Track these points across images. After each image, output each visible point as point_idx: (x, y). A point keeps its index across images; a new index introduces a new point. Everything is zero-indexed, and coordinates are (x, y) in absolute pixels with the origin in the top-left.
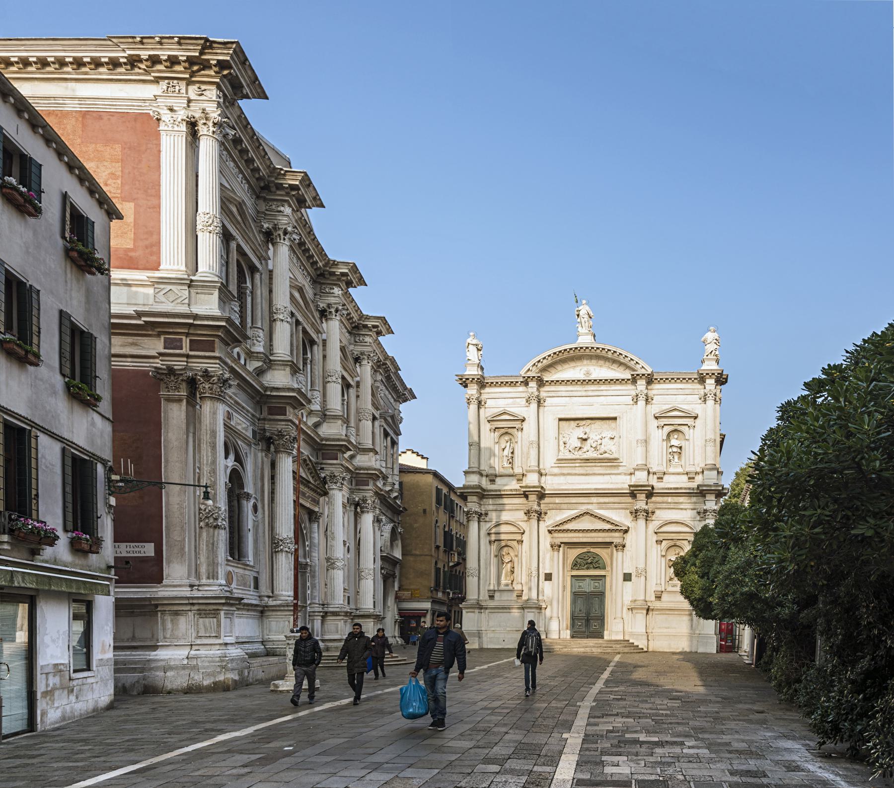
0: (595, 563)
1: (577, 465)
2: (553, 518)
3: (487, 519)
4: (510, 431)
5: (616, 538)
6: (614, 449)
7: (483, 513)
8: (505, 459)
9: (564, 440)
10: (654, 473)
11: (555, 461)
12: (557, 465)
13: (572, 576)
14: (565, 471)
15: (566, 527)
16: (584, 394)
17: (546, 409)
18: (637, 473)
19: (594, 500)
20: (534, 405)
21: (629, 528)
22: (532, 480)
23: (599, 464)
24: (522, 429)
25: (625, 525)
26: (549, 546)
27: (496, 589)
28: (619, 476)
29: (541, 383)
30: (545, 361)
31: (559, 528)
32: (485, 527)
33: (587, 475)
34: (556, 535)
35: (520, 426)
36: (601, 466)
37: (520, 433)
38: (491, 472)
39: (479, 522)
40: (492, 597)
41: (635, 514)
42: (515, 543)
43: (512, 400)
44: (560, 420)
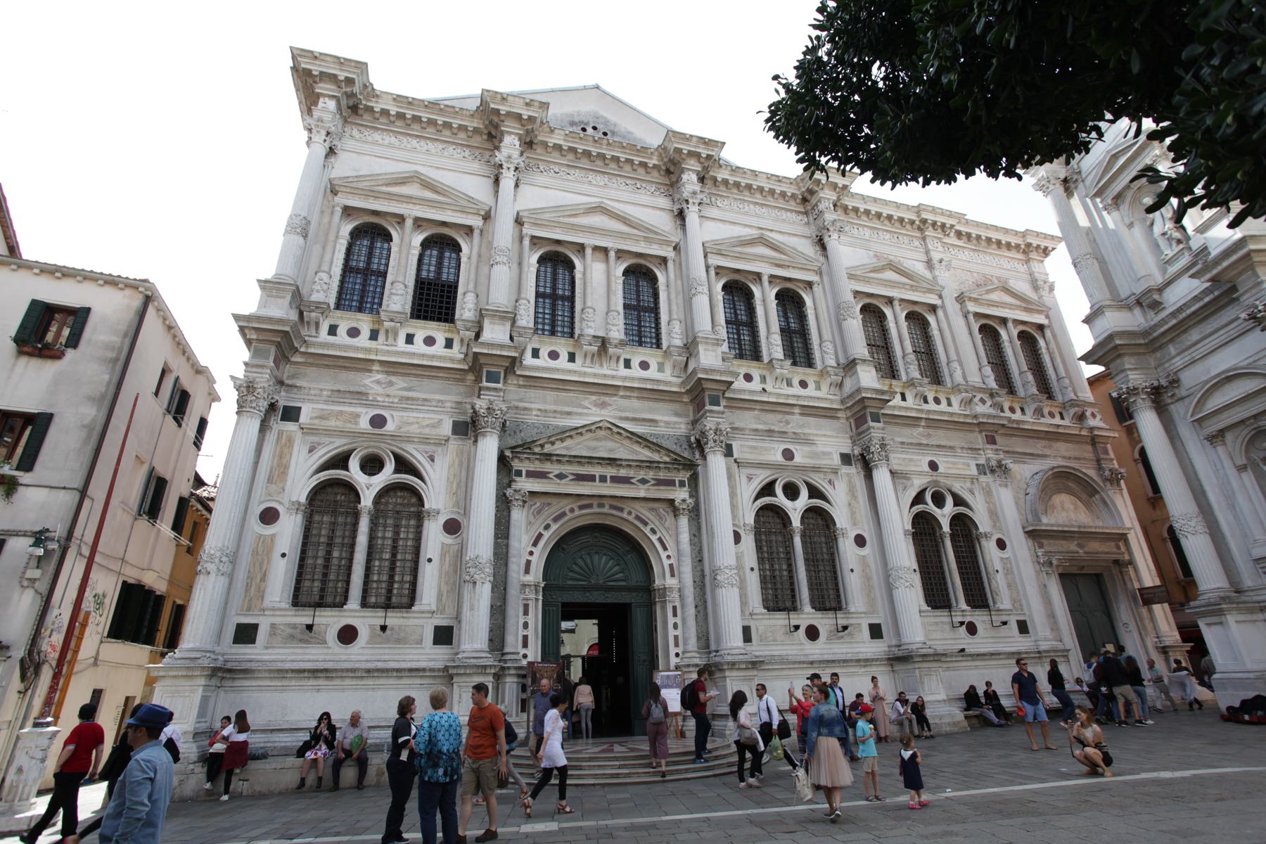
7: (1164, 382)
32: (1181, 412)
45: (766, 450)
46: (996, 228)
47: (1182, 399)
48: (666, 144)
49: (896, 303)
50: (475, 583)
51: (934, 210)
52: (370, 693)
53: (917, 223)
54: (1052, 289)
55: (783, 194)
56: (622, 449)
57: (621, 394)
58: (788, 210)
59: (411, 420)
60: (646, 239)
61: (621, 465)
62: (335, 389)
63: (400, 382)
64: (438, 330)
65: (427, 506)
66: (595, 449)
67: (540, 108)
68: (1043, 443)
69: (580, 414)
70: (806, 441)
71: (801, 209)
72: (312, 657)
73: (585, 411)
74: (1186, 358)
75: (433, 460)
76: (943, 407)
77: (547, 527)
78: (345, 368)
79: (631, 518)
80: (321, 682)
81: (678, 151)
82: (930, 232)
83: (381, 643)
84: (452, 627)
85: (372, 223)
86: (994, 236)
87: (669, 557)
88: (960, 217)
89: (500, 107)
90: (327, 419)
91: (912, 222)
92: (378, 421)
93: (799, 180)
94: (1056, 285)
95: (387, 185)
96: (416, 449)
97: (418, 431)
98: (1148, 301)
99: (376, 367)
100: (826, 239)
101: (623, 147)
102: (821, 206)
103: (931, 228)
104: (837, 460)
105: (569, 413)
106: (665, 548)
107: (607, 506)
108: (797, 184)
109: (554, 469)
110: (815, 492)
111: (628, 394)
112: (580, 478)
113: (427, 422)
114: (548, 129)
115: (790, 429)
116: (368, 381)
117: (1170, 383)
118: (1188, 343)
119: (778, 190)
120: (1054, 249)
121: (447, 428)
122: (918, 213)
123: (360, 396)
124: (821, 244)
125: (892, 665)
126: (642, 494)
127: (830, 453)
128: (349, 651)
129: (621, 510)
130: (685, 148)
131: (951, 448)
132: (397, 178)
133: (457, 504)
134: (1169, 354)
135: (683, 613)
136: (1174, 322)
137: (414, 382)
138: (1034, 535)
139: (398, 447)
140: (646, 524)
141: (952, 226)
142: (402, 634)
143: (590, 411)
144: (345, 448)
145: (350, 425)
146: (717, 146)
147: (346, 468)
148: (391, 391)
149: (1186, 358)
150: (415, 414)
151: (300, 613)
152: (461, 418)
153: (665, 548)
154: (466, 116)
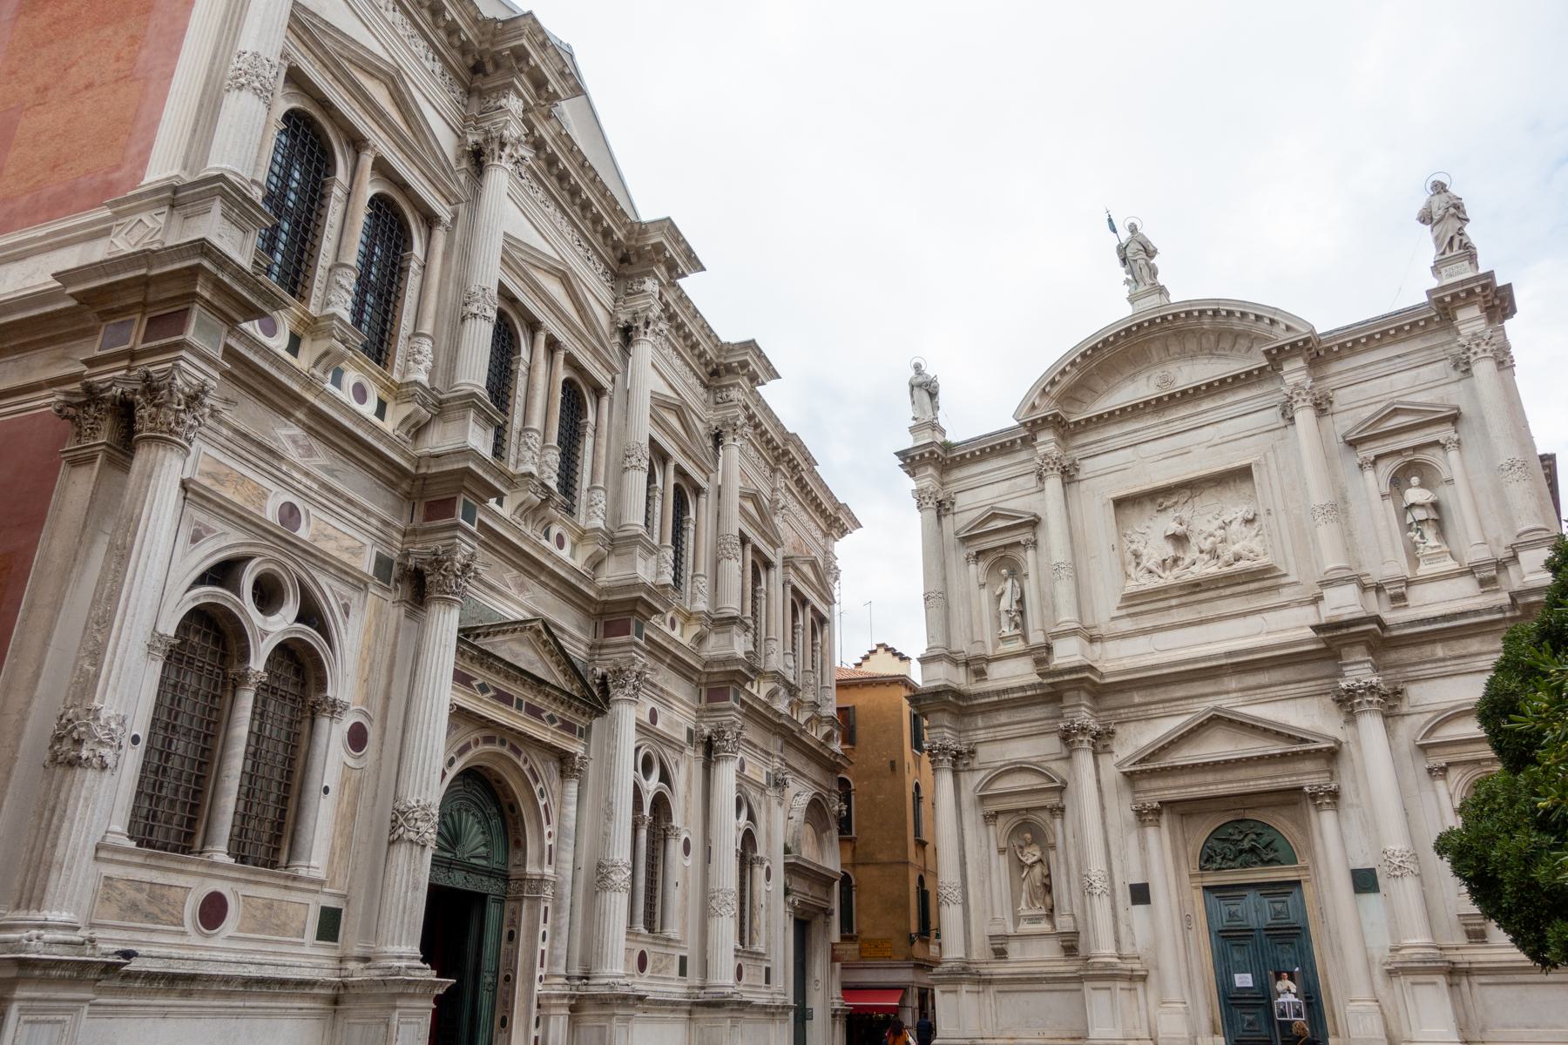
0: (1266, 849)
1: (1174, 602)
2: (1137, 739)
3: (975, 765)
4: (1009, 553)
5: (1309, 777)
6: (1256, 545)
7: (964, 749)
8: (1004, 618)
9: (1134, 547)
10: (1379, 588)
11: (1119, 599)
12: (1124, 612)
13: (1205, 888)
14: (1147, 622)
15: (1167, 761)
16: (1164, 430)
17: (1083, 486)
18: (1329, 593)
19: (1232, 683)
20: (1053, 483)
21: (1340, 744)
22: (1067, 653)
23: (1228, 591)
25: (1326, 738)
26: (1131, 816)
27: (1010, 930)
28: (1285, 613)
29: (1064, 428)
30: (1066, 379)
31: (1151, 766)
32: (971, 781)
33: (1201, 622)
34: (1145, 785)
35: (1029, 536)
36: (1233, 595)
38: (976, 651)
39: (956, 773)
40: (1000, 954)
41: (1347, 702)
42: (1045, 816)
43: (1008, 483)
44: (1120, 503)
46: (826, 489)
47: (973, 770)
48: (649, 227)
49: (749, 547)
50: (424, 846)
51: (801, 447)
52: (233, 1022)
54: (836, 579)
55: (701, 355)
57: (543, 578)
58: (692, 369)
59: (330, 531)
60: (595, 352)
64: (376, 380)
65: (330, 693)
66: (517, 655)
67: (572, 89)
68: (804, 760)
72: (164, 951)
74: (990, 734)
75: (347, 614)
77: (451, 763)
78: (259, 395)
79: (525, 768)
80: (173, 1001)
83: (253, 931)
84: (340, 911)
85: (311, 117)
86: (822, 497)
87: (550, 834)
91: (776, 448)
92: (290, 514)
93: (725, 348)
94: (841, 574)
96: (330, 587)
97: (335, 554)
98: (977, 666)
100: (728, 440)
101: (604, 195)
104: (683, 737)
105: (492, 588)
106: (548, 823)
107: (507, 746)
109: (480, 675)
110: (665, 777)
112: (503, 698)
113: (348, 543)
114: (546, 112)
117: (969, 752)
118: (996, 722)
119: (704, 345)
121: (366, 564)
125: (690, 1012)
126: (547, 737)
127: (679, 724)
128: (210, 943)
129: (518, 753)
130: (670, 250)
131: (755, 746)
132: (370, 63)
133: (366, 700)
135: (554, 919)
136: (996, 699)
137: (338, 463)
138: (792, 869)
139: (309, 574)
140: (537, 781)
142: (283, 918)
147: (237, 590)
149: (990, 734)
150: (333, 522)
151: (153, 862)
152: (386, 552)
153: (548, 823)
154: (469, 14)
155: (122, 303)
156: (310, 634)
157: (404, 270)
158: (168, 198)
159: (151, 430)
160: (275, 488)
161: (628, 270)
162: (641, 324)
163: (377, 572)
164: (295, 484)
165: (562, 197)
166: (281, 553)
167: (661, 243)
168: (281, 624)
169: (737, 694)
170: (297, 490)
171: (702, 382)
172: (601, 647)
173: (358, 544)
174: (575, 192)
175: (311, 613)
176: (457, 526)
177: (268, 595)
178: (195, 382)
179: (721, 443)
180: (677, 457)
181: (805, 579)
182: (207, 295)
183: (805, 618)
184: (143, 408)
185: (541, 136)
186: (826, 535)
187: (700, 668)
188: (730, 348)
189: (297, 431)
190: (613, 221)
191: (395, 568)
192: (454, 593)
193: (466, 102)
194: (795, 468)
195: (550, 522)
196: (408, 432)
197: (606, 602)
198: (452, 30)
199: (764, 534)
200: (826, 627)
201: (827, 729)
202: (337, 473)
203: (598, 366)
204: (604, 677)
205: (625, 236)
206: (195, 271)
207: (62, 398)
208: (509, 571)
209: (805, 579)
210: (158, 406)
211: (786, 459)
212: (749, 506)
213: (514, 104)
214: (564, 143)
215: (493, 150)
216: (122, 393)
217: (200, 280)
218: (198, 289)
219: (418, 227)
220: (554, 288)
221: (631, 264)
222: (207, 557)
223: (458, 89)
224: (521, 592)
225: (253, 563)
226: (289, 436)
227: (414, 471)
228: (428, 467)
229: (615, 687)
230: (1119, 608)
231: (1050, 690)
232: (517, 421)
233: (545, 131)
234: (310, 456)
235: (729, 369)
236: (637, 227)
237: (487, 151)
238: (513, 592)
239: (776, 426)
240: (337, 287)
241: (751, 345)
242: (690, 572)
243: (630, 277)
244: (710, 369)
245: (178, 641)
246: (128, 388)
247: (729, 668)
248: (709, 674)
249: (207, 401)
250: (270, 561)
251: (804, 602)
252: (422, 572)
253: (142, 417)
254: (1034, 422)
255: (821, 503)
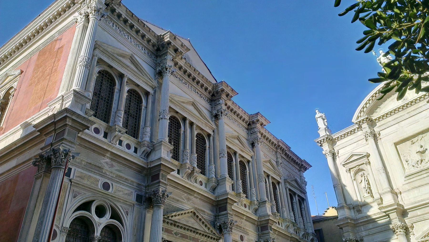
8: (364, 190)
9: (406, 158)
12: (407, 182)
16: (408, 116)
20: (371, 140)
24: (369, 163)
37: (368, 166)
45: (236, 234)
48: (218, 84)
49: (270, 177)
51: (284, 143)
53: (277, 145)
56: (196, 224)
59: (120, 189)
61: (197, 233)
62: (89, 162)
63: (117, 166)
66: (188, 222)
69: (181, 202)
70: (247, 234)
71: (247, 127)
73: (183, 201)
75: (128, 215)
76: (280, 226)
78: (94, 151)
81: (223, 90)
82: (279, 150)
86: (295, 158)
88: (289, 148)
89: (172, 42)
90: (83, 179)
91: (275, 145)
92: (106, 186)
93: (251, 116)
95: (117, 54)
96: (121, 206)
97: (123, 196)
99: (108, 155)
102: (256, 130)
103: (280, 149)
105: (178, 200)
108: (249, 117)
109: (175, 229)
111: (197, 196)
113: (126, 192)
115: (242, 225)
116: (103, 161)
120: (308, 169)
122: (278, 142)
123: (98, 169)
124: (253, 145)
134: (361, 230)
136: (366, 219)
141: (286, 150)
143: (184, 201)
144: (91, 199)
145: (93, 185)
146: (235, 94)
147: (89, 210)
148: (113, 169)
150: (121, 186)
152: (140, 193)
155: (50, 131)
156: (115, 222)
157: (140, 109)
158: (61, 99)
159: (55, 165)
160: (101, 178)
161: (214, 98)
162: (220, 113)
163: (137, 200)
164: (108, 176)
165: (190, 81)
166: (104, 198)
167: (223, 88)
168: (106, 220)
169: (271, 227)
170: (109, 178)
171: (246, 128)
172: (218, 216)
173: (131, 192)
174: (194, 79)
175: (115, 216)
176: (159, 182)
177: (101, 212)
178: (67, 149)
179: (254, 145)
180: (239, 152)
181: (292, 186)
182: (70, 124)
183: (296, 199)
184: (53, 159)
185: (180, 65)
186: (299, 171)
187: (256, 219)
188: (251, 116)
189: (108, 160)
190: (207, 85)
191: (144, 199)
192: (160, 203)
193: (156, 60)
194: (283, 150)
195: (196, 177)
196: (145, 156)
197: (218, 201)
198: (149, 41)
199: (275, 173)
200: (305, 202)
201: (311, 237)
202: (122, 171)
203: (208, 128)
204: (220, 226)
205: (212, 89)
206: (66, 117)
207: (35, 160)
208: (183, 195)
209: (292, 186)
210: (56, 158)
211: (279, 148)
212: (268, 164)
213: (169, 57)
214: (188, 66)
215: (164, 71)
216: (48, 156)
217: (68, 119)
218: (67, 123)
219: (144, 96)
220: (191, 108)
221: (215, 96)
222: (79, 202)
223: (153, 56)
224: (188, 201)
225: (94, 203)
226: (105, 162)
227: (146, 167)
228: (150, 165)
229: (224, 229)
230: (405, 181)
231: (384, 214)
232: (181, 147)
233: (181, 63)
234: (112, 167)
235: (253, 122)
236: (215, 85)
237: (163, 72)
238: (186, 201)
239: (274, 138)
240: (117, 117)
241: (257, 114)
242: (249, 188)
243: (215, 100)
244: (247, 124)
245: (70, 229)
246: (49, 154)
247: (266, 219)
248: (260, 221)
249: (71, 154)
250: (100, 201)
251: (295, 194)
252: (151, 197)
253: (53, 162)
254: (360, 122)
255: (295, 160)
